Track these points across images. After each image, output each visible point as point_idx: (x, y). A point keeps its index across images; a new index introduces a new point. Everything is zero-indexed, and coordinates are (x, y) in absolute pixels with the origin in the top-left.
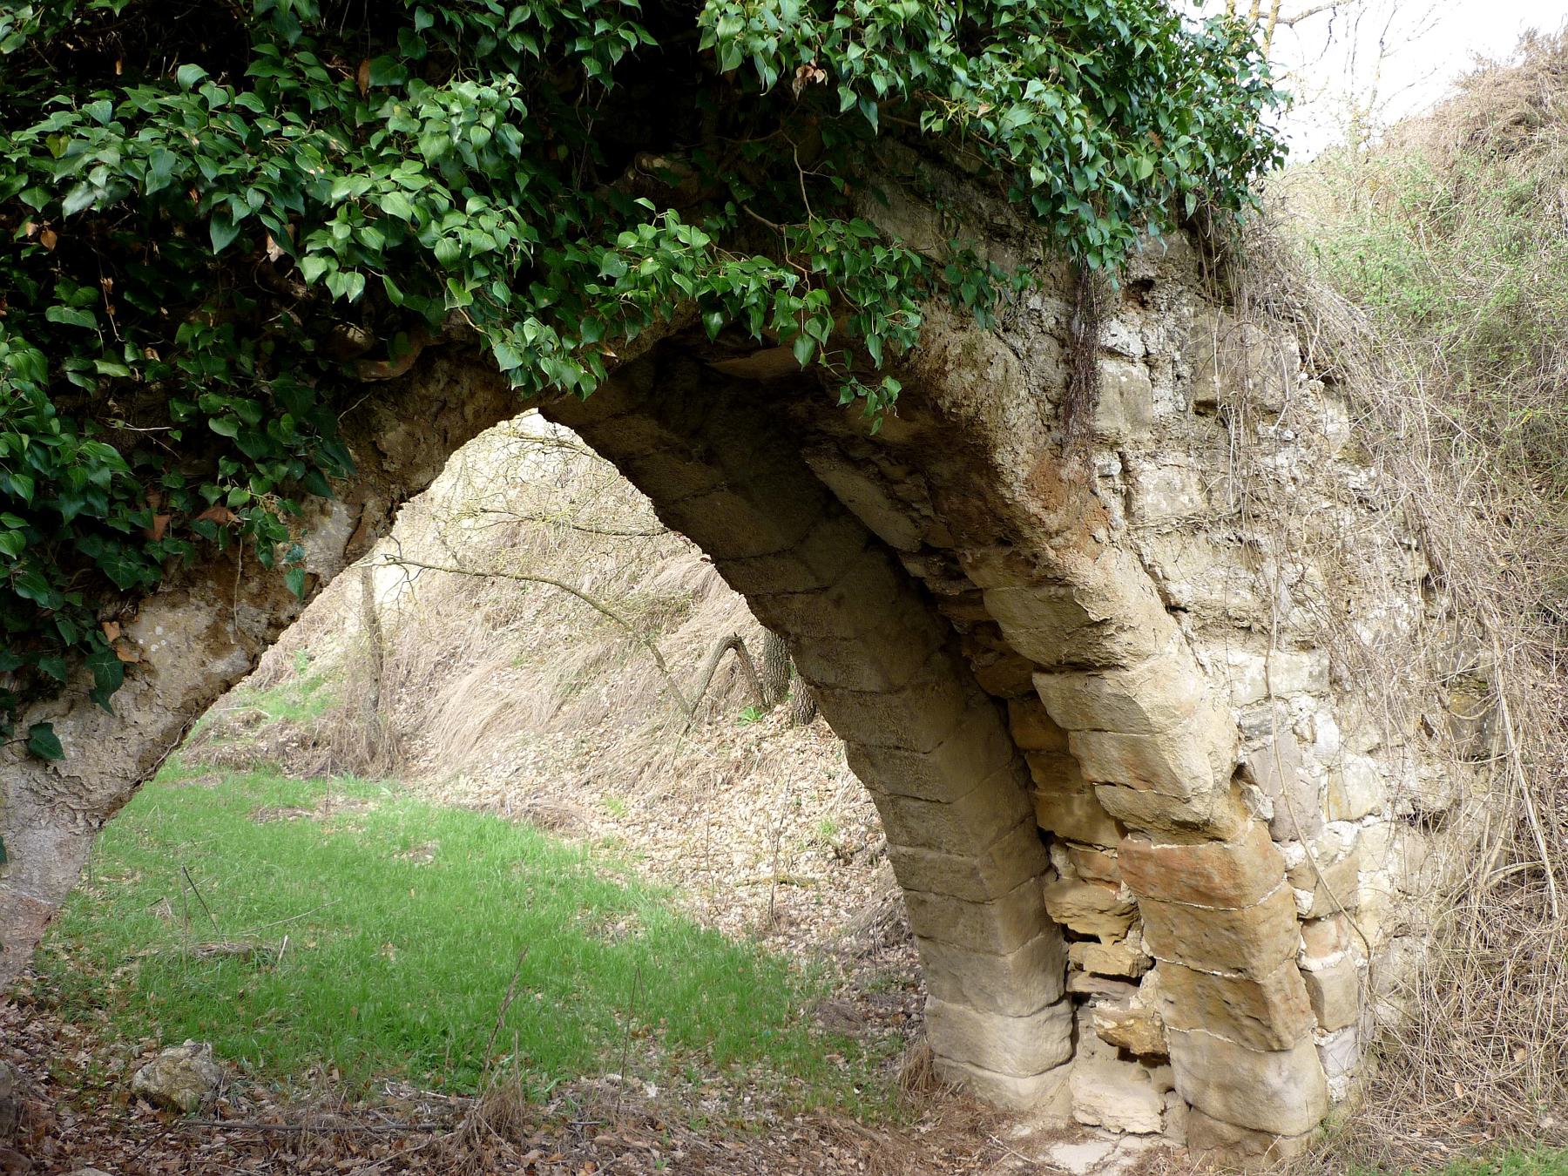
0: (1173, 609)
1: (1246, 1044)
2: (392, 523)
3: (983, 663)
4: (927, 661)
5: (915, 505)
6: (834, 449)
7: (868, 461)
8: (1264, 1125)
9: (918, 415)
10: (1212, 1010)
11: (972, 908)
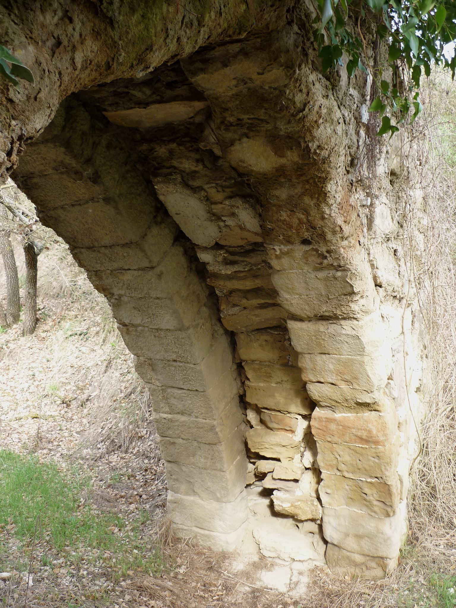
0: (378, 285)
1: (373, 514)
2: (340, 77)
3: (230, 313)
4: (199, 312)
5: (223, 218)
6: (179, 179)
7: (201, 188)
8: (380, 554)
9: (289, 153)
10: (352, 497)
11: (207, 447)
